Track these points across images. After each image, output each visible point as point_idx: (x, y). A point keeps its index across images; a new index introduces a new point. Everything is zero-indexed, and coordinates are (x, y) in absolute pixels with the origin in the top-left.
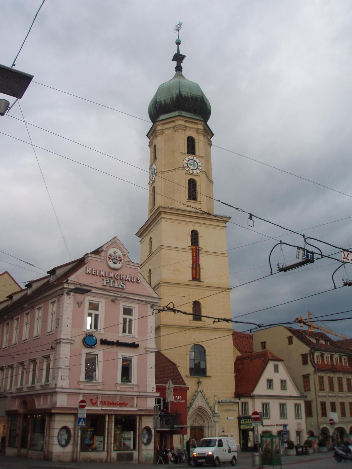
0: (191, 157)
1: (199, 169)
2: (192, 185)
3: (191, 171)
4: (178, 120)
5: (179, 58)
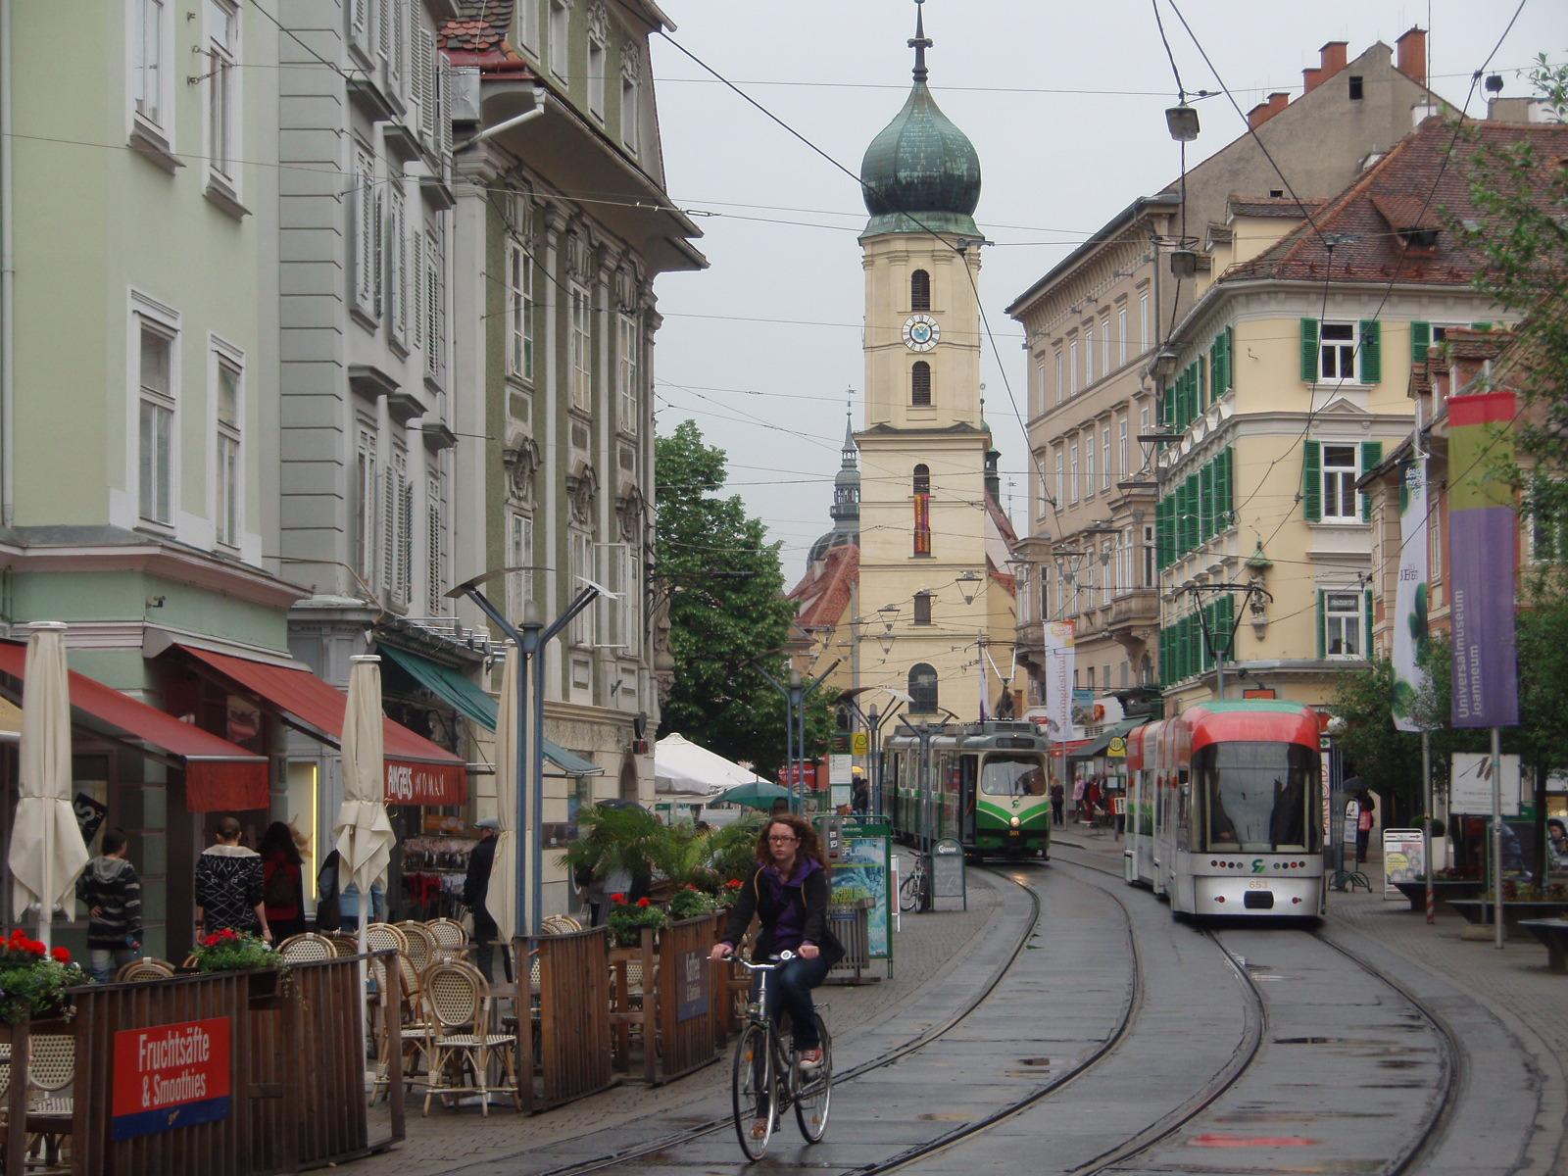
0: (917, 318)
1: (934, 340)
2: (921, 374)
3: (917, 348)
4: (894, 239)
5: (920, 44)
